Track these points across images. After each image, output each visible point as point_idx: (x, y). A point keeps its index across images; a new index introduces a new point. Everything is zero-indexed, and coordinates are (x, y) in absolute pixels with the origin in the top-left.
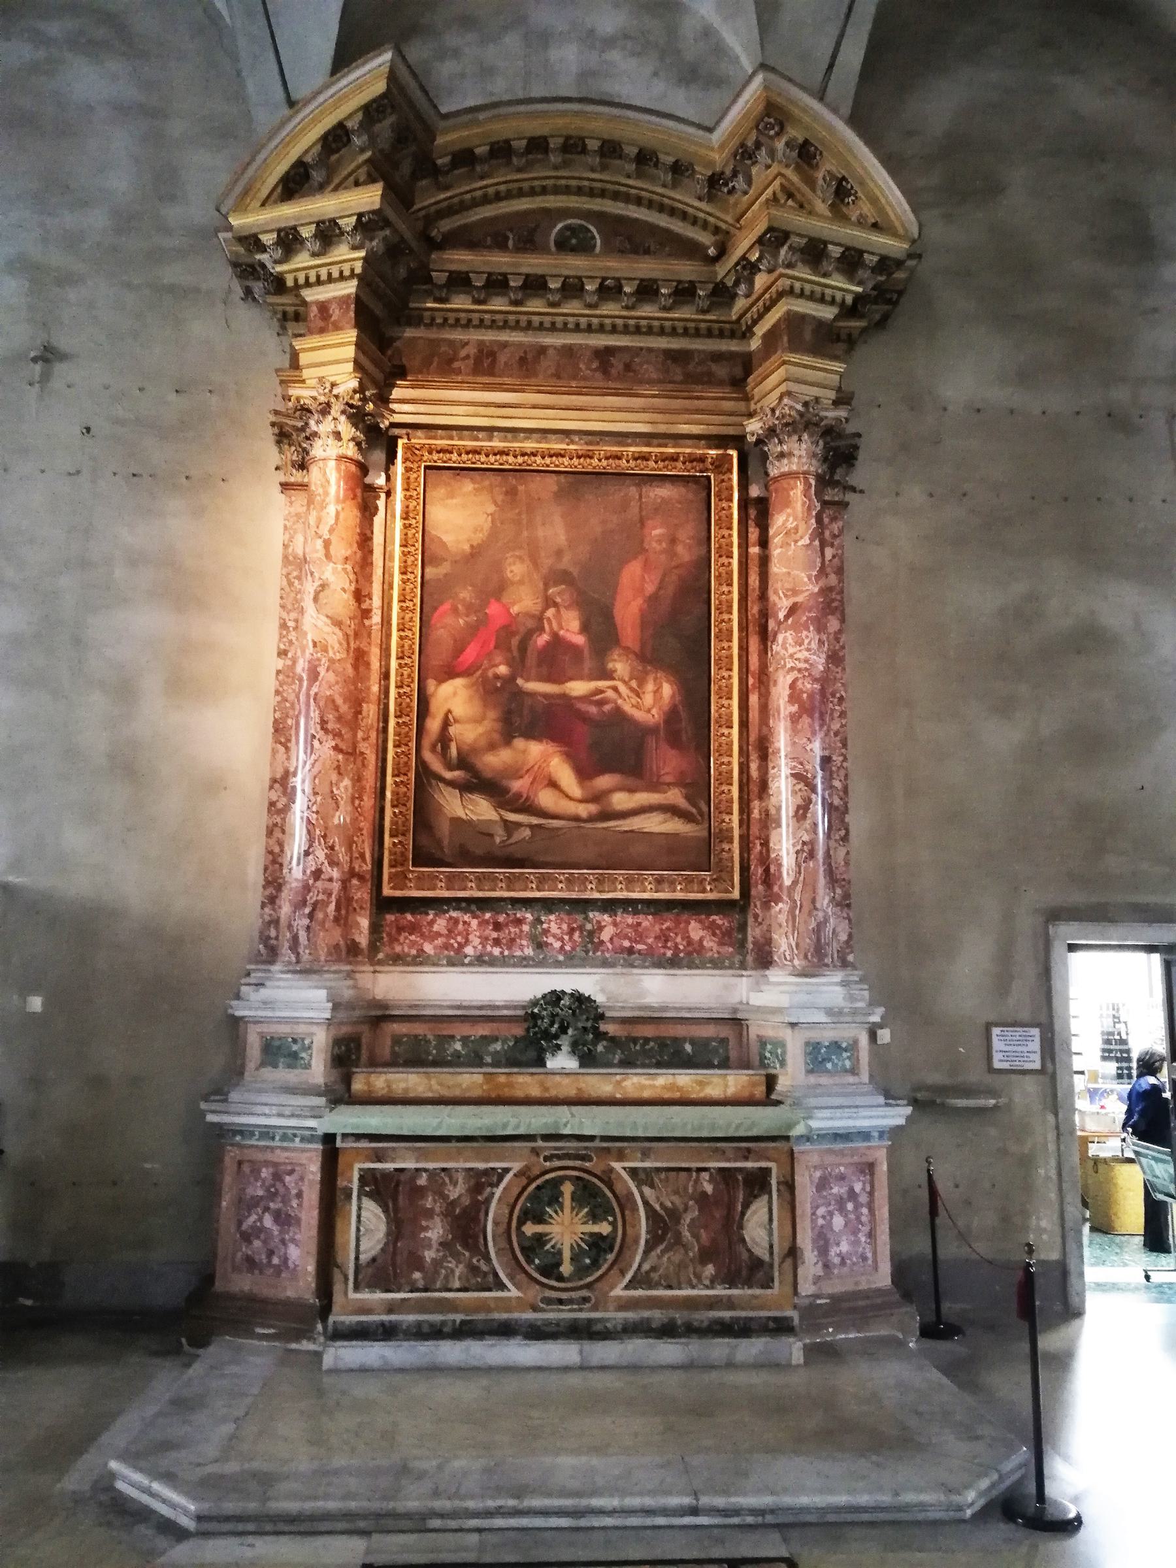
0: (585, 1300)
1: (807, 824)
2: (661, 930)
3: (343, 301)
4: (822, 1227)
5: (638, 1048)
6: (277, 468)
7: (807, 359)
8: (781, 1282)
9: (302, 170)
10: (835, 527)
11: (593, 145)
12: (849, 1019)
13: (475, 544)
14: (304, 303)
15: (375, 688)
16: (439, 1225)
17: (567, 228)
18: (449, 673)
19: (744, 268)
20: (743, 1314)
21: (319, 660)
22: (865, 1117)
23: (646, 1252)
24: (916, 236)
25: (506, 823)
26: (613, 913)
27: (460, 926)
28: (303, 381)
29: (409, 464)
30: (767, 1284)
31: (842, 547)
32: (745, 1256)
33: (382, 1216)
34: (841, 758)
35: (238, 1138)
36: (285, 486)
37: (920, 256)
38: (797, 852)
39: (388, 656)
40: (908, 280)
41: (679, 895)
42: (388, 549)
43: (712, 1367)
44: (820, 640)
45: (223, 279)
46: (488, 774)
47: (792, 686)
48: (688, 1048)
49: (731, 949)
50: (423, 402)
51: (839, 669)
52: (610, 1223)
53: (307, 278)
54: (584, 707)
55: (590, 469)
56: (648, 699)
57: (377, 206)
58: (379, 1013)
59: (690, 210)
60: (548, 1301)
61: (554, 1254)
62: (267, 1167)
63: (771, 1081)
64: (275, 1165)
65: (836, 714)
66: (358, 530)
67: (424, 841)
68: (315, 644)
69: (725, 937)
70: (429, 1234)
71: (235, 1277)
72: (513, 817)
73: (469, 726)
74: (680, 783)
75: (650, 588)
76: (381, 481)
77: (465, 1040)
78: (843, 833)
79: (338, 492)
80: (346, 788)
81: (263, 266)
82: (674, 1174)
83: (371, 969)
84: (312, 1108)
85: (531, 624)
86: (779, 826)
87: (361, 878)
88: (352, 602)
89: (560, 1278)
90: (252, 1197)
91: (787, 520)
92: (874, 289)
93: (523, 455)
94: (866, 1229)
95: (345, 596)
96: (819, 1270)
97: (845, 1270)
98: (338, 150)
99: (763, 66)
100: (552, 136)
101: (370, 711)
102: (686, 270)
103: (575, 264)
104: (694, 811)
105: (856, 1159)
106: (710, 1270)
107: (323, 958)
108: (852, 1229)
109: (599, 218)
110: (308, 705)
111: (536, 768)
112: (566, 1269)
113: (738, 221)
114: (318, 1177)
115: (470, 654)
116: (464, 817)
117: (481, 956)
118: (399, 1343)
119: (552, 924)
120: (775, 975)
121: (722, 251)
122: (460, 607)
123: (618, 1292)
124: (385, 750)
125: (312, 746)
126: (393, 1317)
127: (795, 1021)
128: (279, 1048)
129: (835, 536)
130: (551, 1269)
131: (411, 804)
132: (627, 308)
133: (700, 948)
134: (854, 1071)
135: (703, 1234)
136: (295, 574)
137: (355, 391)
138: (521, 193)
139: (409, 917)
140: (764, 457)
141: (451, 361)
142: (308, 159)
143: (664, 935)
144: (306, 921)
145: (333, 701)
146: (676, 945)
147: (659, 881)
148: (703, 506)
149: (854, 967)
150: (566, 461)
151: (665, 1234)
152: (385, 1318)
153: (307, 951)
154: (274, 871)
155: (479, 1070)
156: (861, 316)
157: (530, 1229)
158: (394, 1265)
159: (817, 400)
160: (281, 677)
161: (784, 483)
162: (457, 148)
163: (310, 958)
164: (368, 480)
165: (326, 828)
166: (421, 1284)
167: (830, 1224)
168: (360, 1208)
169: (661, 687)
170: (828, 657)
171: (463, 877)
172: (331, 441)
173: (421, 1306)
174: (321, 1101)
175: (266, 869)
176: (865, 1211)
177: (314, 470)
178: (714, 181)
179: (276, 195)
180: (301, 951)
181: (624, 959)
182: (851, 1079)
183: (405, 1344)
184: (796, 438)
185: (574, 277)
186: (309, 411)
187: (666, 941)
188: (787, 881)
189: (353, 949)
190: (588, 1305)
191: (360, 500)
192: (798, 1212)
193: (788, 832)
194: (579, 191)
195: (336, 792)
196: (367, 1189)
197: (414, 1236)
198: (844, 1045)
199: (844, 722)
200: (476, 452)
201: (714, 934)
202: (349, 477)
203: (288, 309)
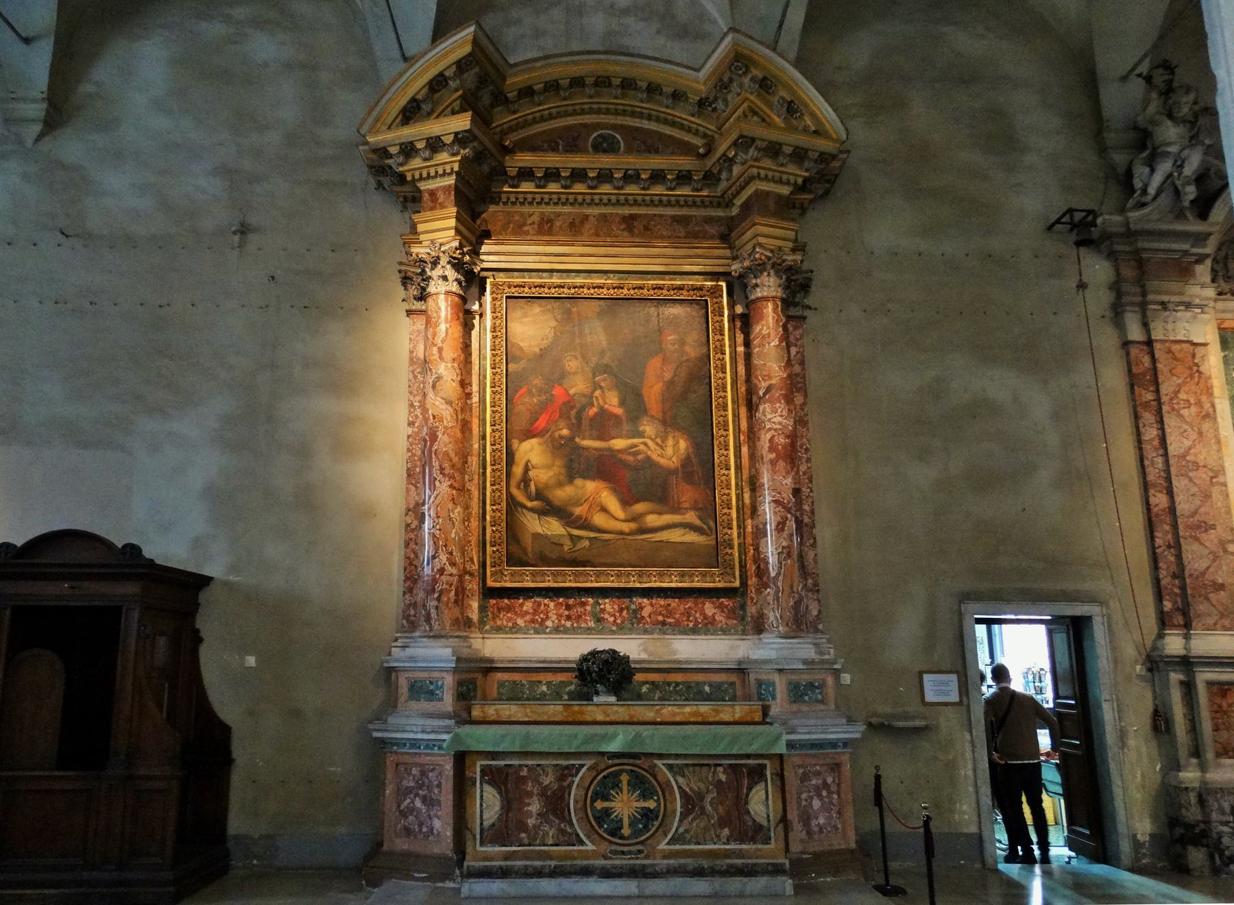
0: (640, 852)
1: (785, 534)
2: (685, 609)
3: (446, 189)
4: (805, 806)
5: (671, 689)
6: (403, 300)
7: (772, 221)
8: (775, 840)
9: (415, 104)
10: (798, 333)
11: (616, 82)
12: (819, 667)
13: (542, 347)
14: (420, 191)
15: (476, 446)
16: (537, 802)
18: (529, 434)
19: (725, 161)
20: (750, 861)
21: (437, 427)
22: (832, 733)
23: (681, 821)
24: (844, 136)
25: (571, 536)
27: (542, 607)
28: (421, 243)
29: (495, 295)
30: (767, 841)
31: (802, 346)
32: (750, 823)
33: (498, 796)
34: (809, 490)
35: (395, 748)
37: (849, 152)
38: (779, 553)
39: (484, 424)
40: (841, 168)
42: (482, 353)
43: (730, 896)
44: (789, 410)
45: (359, 174)
46: (557, 502)
47: (771, 440)
48: (707, 689)
49: (735, 622)
50: (504, 254)
51: (805, 430)
52: (655, 800)
53: (421, 175)
55: (622, 296)
56: (669, 451)
57: (468, 127)
58: (489, 666)
59: (686, 123)
60: (615, 852)
61: (617, 822)
62: (416, 767)
63: (765, 711)
64: (422, 765)
65: (804, 460)
66: (461, 341)
67: (513, 548)
68: (434, 417)
69: (731, 614)
70: (530, 808)
71: (398, 841)
73: (544, 471)
75: (668, 376)
76: (476, 307)
77: (549, 684)
78: (812, 541)
79: (446, 315)
80: (459, 513)
81: (390, 167)
82: (697, 768)
83: (481, 636)
84: (446, 727)
85: (584, 400)
86: (766, 536)
87: (471, 574)
88: (459, 388)
89: (622, 837)
90: (407, 788)
91: (762, 329)
92: (817, 173)
93: (575, 288)
94: (835, 809)
95: (454, 384)
96: (804, 835)
97: (822, 836)
98: (439, 90)
99: (731, 29)
100: (587, 76)
102: (685, 163)
103: (606, 161)
104: (705, 527)
105: (828, 761)
106: (726, 831)
107: (448, 628)
108: (826, 808)
110: (431, 458)
111: (591, 499)
112: (626, 831)
113: (720, 129)
114: (452, 773)
115: (541, 423)
116: (542, 532)
117: (558, 627)
118: (512, 880)
119: (607, 605)
120: (767, 638)
121: (709, 151)
122: (534, 390)
123: (663, 846)
124: (484, 488)
125: (435, 485)
126: (509, 863)
127: (781, 667)
128: (421, 687)
129: (797, 340)
130: (615, 831)
131: (504, 524)
132: (644, 189)
134: (822, 702)
135: (721, 809)
136: (418, 370)
137: (456, 249)
138: (567, 114)
139: (506, 601)
140: (745, 286)
141: (521, 226)
142: (420, 97)
143: (687, 612)
144: (435, 603)
145: (448, 454)
146: (696, 618)
147: (682, 575)
148: (703, 320)
149: (823, 633)
150: (605, 291)
151: (693, 808)
152: (503, 863)
153: (437, 623)
154: (410, 572)
155: (559, 702)
156: (810, 192)
157: (599, 805)
158: (506, 827)
159: (780, 248)
160: (411, 440)
161: (759, 304)
162: (522, 86)
163: (440, 628)
164: (467, 307)
165: (446, 540)
166: (526, 841)
167: (811, 803)
168: (482, 791)
169: (678, 442)
170: (795, 422)
171: (544, 574)
172: (440, 282)
173: (525, 855)
174: (451, 722)
175: (405, 570)
176: (835, 796)
177: (430, 301)
178: (701, 103)
179: (398, 121)
180: (433, 623)
181: (660, 630)
182: (822, 707)
183: (517, 880)
184: (766, 274)
185: (607, 169)
186: (426, 263)
187: (689, 617)
188: (773, 574)
189: (468, 623)
190: (642, 855)
191: (462, 320)
192: (788, 796)
193: (772, 540)
194: (608, 112)
195: (452, 516)
196: (487, 778)
197: (520, 810)
198: (817, 684)
199: (809, 465)
201: (723, 611)
202: (454, 306)
203: (407, 194)
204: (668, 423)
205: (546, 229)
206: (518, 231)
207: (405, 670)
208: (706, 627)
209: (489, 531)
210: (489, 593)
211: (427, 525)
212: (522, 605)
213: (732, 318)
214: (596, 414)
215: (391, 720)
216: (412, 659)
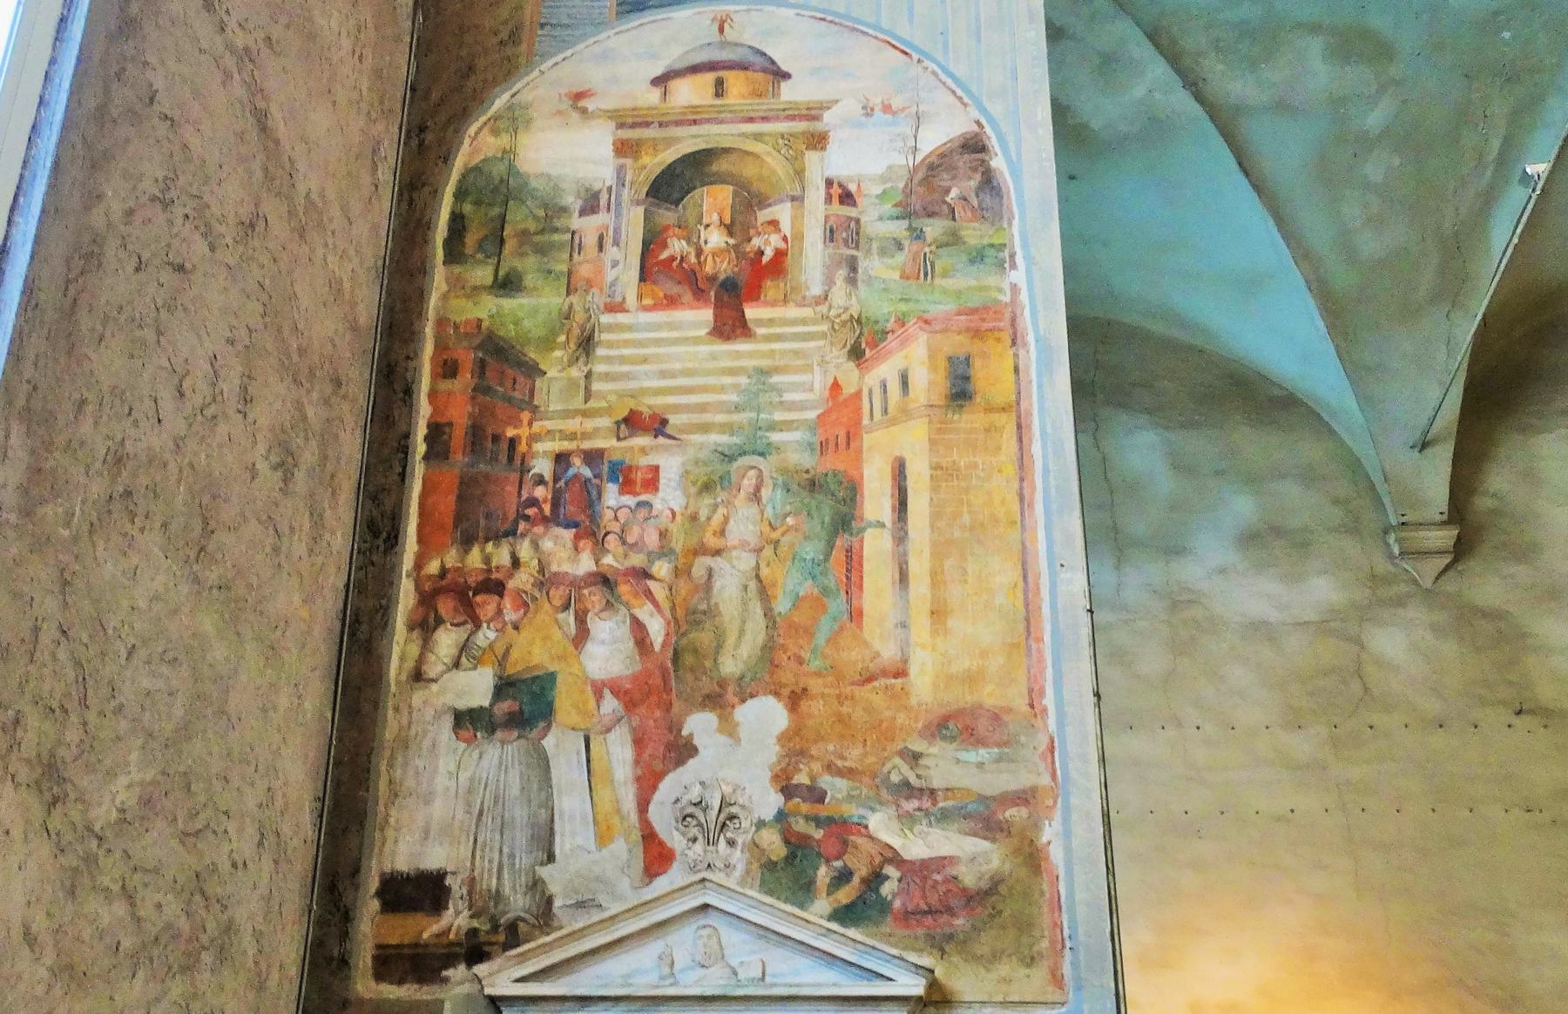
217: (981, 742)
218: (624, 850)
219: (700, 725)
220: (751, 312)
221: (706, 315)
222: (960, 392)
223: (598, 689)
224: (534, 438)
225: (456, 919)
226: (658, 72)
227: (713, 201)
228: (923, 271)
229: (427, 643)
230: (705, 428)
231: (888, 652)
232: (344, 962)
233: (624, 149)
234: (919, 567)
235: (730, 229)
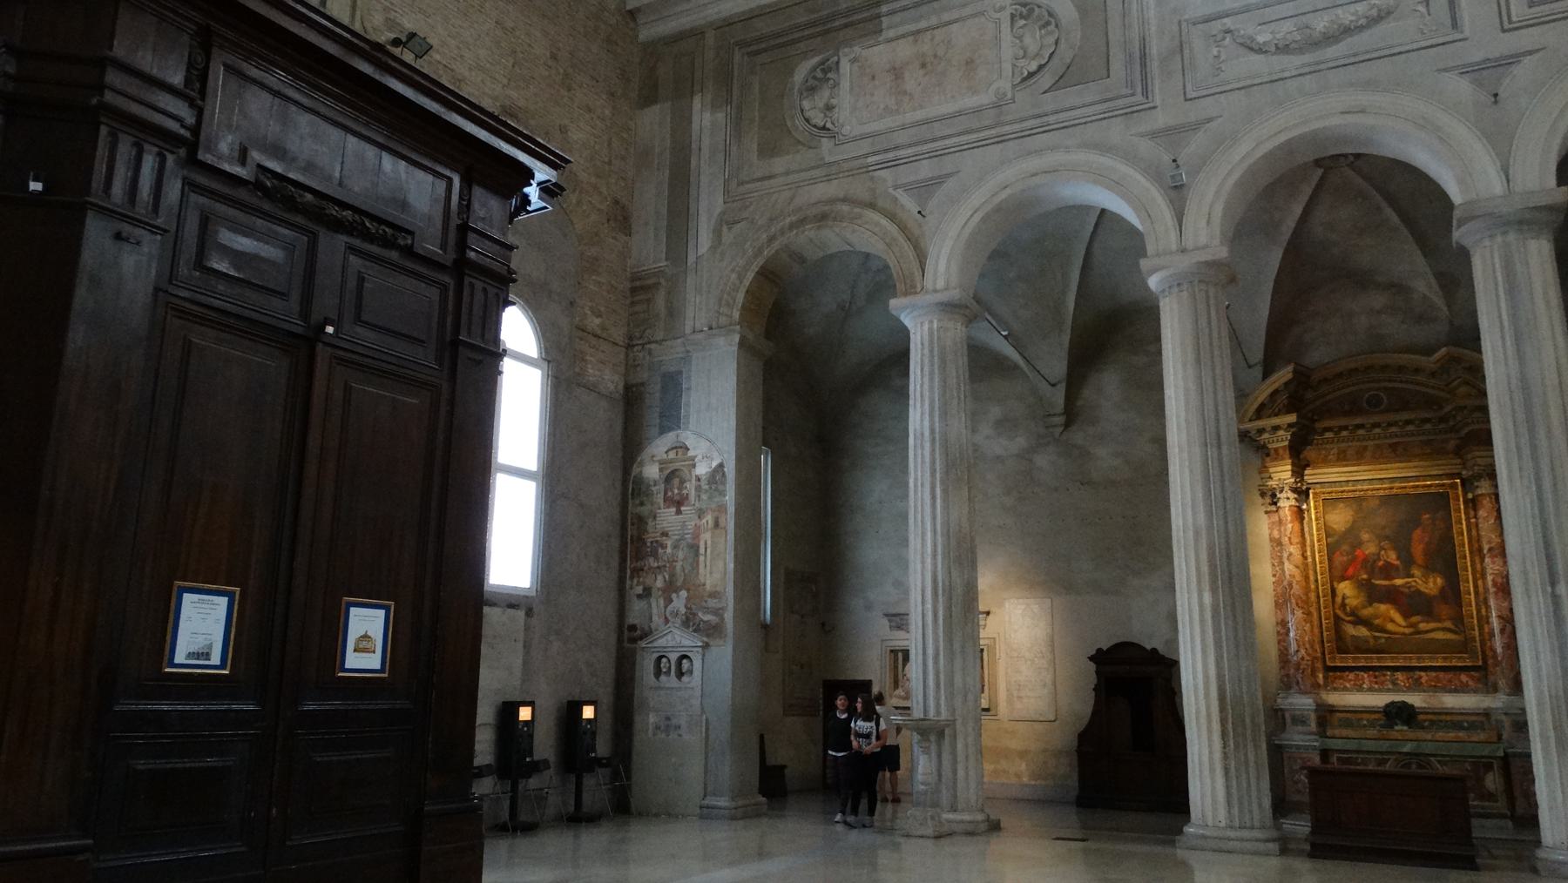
17: (1370, 396)
18: (1343, 578)
25: (1375, 637)
26: (1426, 671)
36: (1266, 512)
41: (1454, 664)
54: (1402, 589)
56: (1431, 585)
72: (1377, 634)
74: (1450, 619)
75: (1426, 539)
76: (1305, 507)
77: (1368, 720)
85: (1376, 557)
101: (1313, 596)
109: (1386, 389)
115: (1351, 571)
133: (1467, 686)
189: (1319, 686)
200: (1342, 492)
204: (1429, 568)
205: (1342, 459)
206: (1326, 462)
207: (1287, 710)
208: (1462, 689)
209: (1325, 634)
210: (1328, 669)
211: (1292, 634)
212: (1348, 676)
213: (1466, 502)
214: (1384, 565)
215: (1283, 735)
216: (1291, 704)
217: (715, 597)
218: (662, 620)
219: (674, 596)
220: (682, 508)
221: (674, 509)
222: (717, 525)
223: (659, 589)
224: (648, 538)
225: (639, 632)
226: (665, 450)
227: (676, 481)
228: (710, 498)
229: (632, 582)
230: (675, 535)
231: (703, 581)
232: (623, 641)
233: (661, 470)
234: (708, 564)
235: (678, 489)
